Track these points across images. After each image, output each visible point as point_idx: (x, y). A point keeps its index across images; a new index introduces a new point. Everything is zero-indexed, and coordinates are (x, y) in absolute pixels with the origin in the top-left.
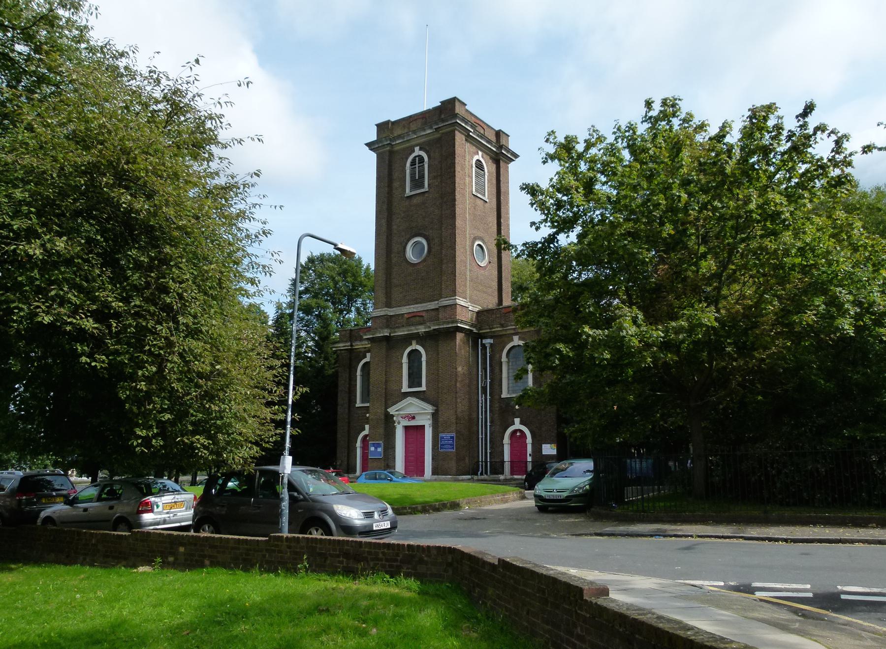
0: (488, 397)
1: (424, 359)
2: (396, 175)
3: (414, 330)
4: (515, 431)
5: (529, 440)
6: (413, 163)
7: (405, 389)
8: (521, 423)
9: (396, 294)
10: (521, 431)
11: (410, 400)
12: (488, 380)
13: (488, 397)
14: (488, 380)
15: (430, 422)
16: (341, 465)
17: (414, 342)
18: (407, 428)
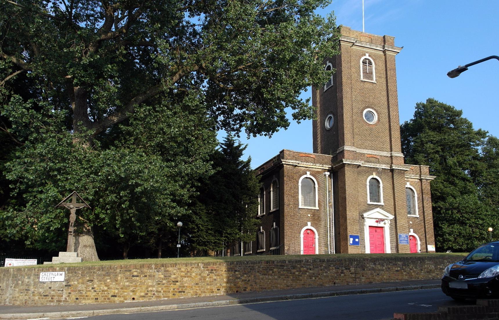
1: (381, 185)
3: (378, 166)
7: (369, 202)
11: (378, 209)
16: (288, 250)
17: (374, 173)
18: (370, 226)
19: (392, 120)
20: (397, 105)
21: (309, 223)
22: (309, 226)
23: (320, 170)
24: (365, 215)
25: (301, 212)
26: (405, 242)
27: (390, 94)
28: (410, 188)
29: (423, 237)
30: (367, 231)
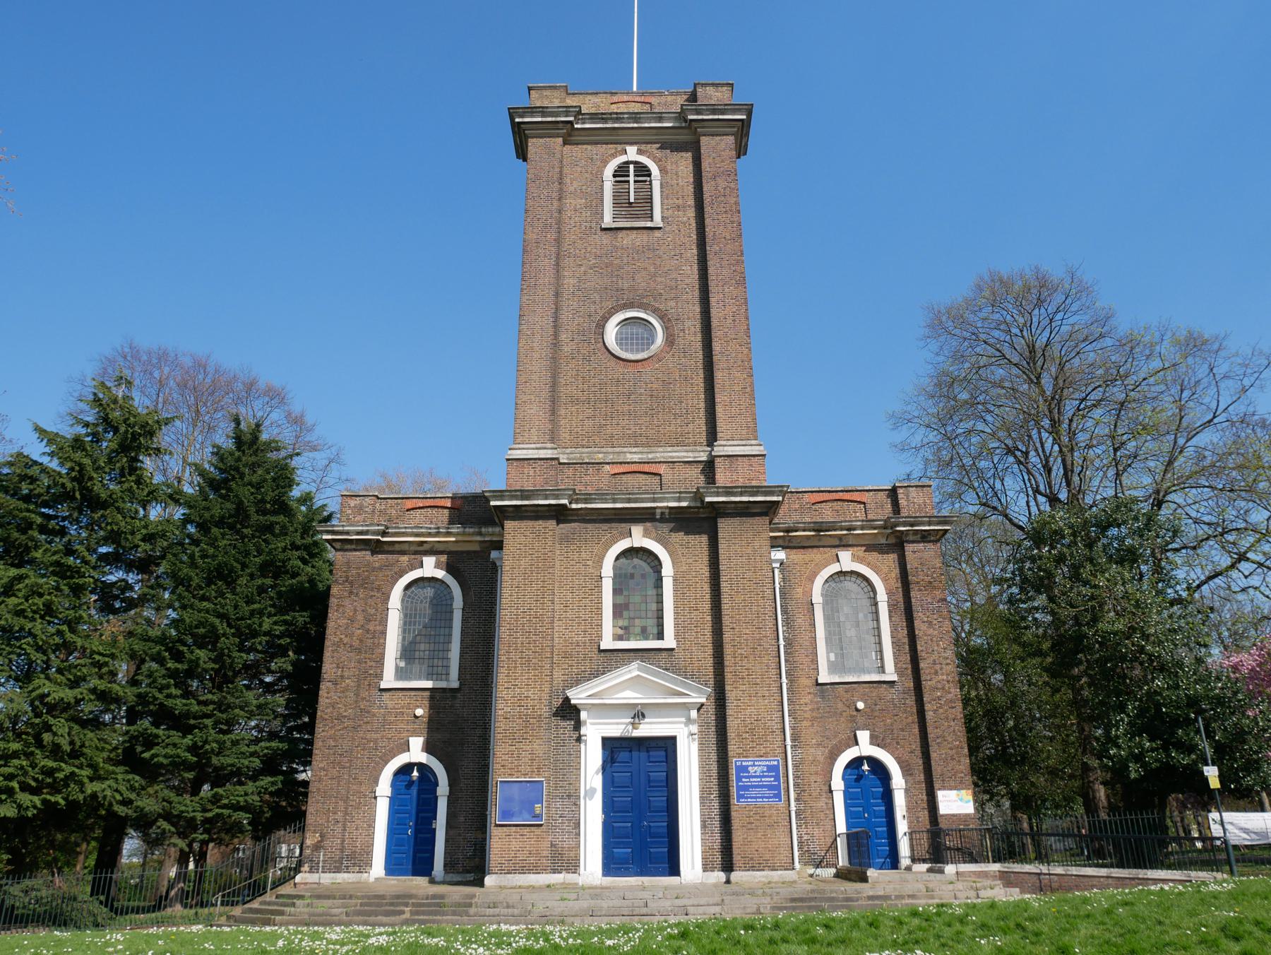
0: (784, 680)
1: (667, 570)
2: (572, 185)
4: (856, 763)
5: (898, 781)
6: (621, 172)
7: (607, 643)
8: (874, 741)
9: (569, 419)
10: (873, 761)
11: (633, 670)
12: (782, 642)
13: (784, 680)
14: (782, 642)
15: (694, 728)
16: (317, 847)
19: (717, 334)
20: (742, 282)
21: (417, 743)
22: (416, 752)
23: (476, 548)
24: (578, 696)
25: (390, 704)
26: (766, 792)
27: (711, 249)
28: (852, 572)
29: (918, 762)
30: (592, 756)
